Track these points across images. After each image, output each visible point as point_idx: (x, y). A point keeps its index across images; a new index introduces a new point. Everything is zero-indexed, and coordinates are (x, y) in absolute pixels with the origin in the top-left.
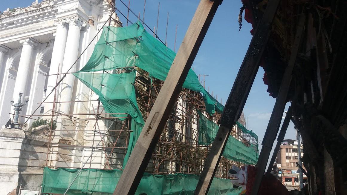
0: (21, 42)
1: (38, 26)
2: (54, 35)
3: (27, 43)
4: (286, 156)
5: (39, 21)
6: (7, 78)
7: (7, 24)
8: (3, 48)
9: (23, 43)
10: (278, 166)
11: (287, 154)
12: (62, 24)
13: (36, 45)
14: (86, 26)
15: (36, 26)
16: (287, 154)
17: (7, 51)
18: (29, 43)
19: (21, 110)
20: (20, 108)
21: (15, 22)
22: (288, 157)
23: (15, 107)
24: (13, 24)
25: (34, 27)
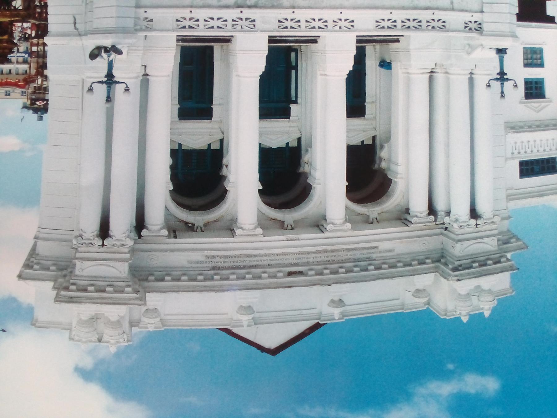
1: (215, 260)
5: (213, 268)
9: (255, 228)
15: (222, 260)
24: (290, 274)
25: (227, 260)
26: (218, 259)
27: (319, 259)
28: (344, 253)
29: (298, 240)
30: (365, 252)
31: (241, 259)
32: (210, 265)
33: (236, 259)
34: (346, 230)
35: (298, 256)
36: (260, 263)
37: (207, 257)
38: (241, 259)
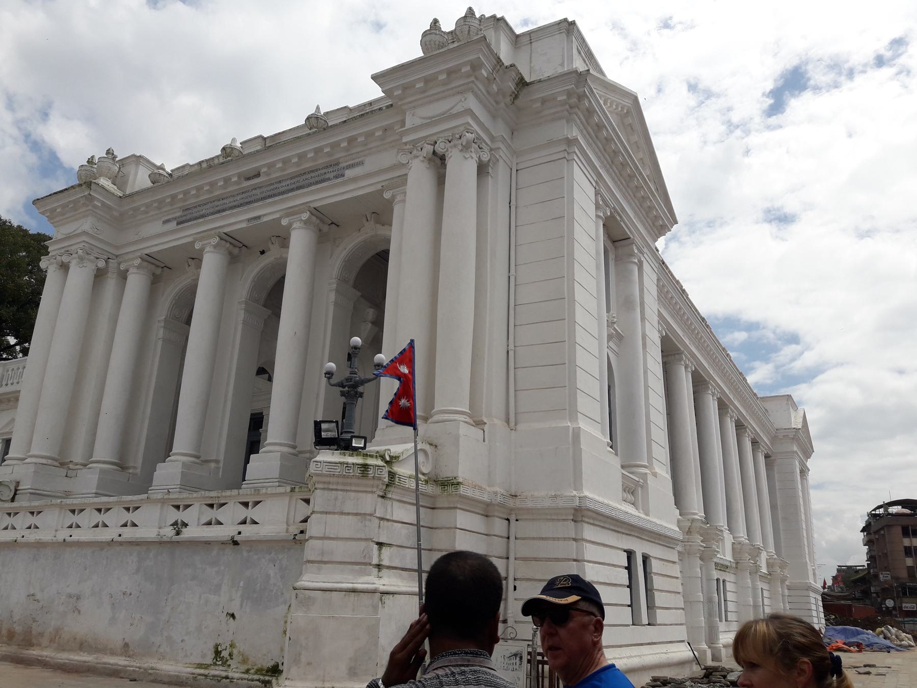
0: (284, 222)
2: (387, 195)
3: (302, 225)
4: (906, 548)
6: (240, 327)
7: (239, 177)
8: (228, 245)
9: (290, 225)
10: (881, 576)
11: (907, 542)
12: (421, 158)
13: (325, 228)
14: (489, 161)
15: (327, 176)
16: (907, 542)
17: (236, 251)
18: (306, 222)
19: (361, 395)
20: (360, 389)
21: (264, 170)
22: (908, 551)
23: (341, 389)
24: (258, 175)
26: (331, 175)
27: (231, 199)
28: (208, 212)
29: (249, 220)
30: (188, 217)
31: (307, 182)
32: (342, 165)
33: (312, 181)
34: (201, 239)
35: (249, 199)
36: (288, 182)
37: (343, 175)
38: (307, 182)
